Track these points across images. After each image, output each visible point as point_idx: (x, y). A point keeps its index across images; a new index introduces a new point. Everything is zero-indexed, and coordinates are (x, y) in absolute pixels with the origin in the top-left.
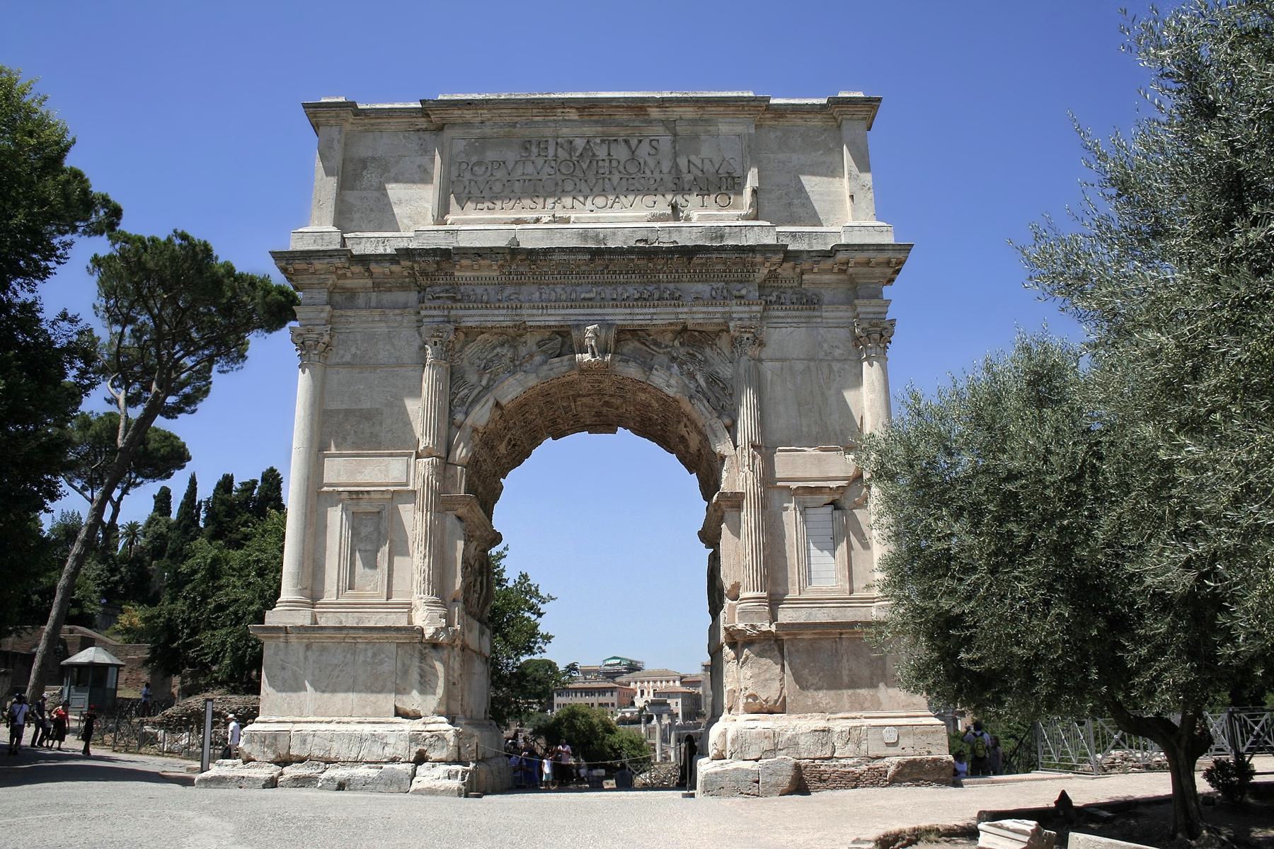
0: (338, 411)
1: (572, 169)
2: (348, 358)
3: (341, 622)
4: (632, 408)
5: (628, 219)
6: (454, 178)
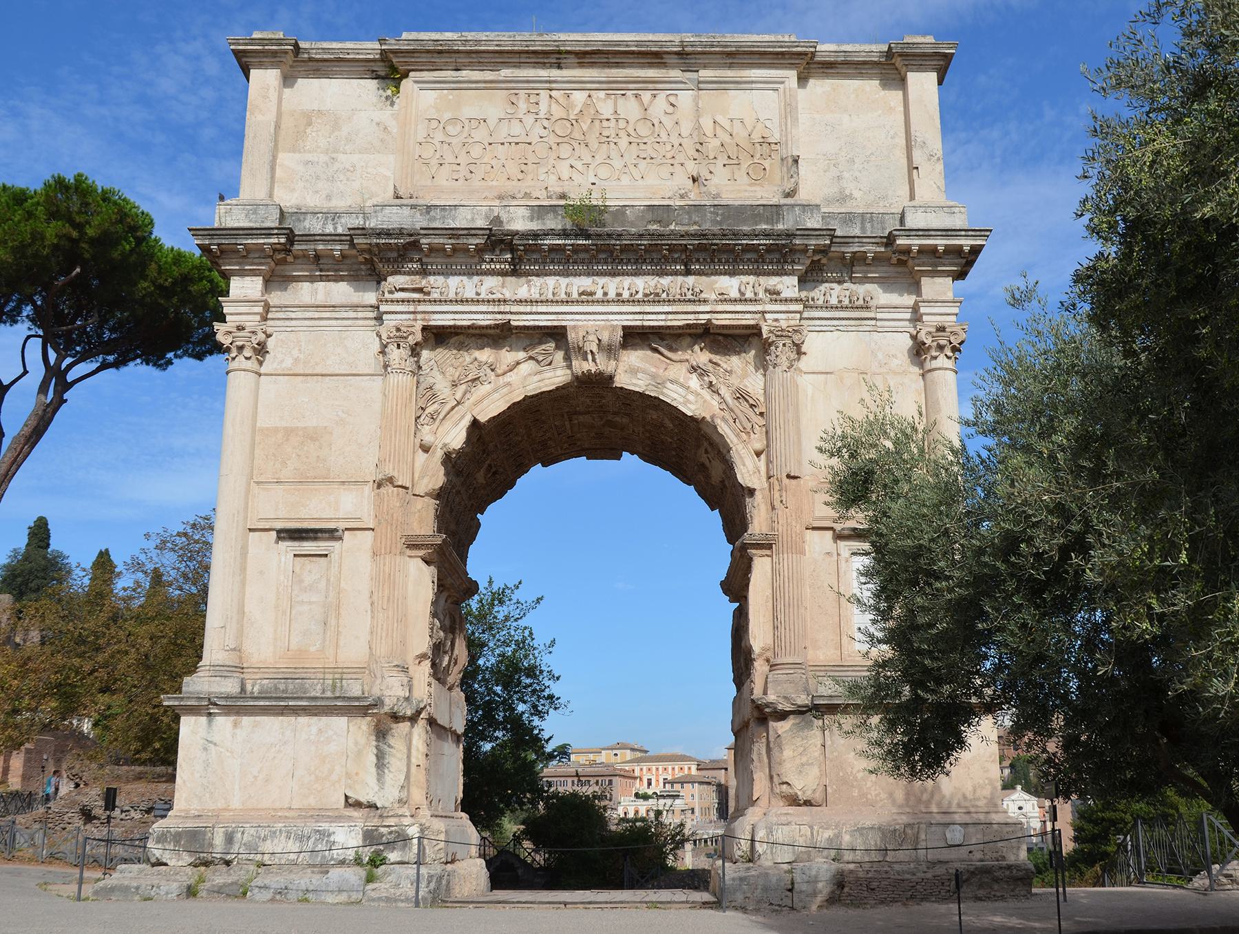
0: (276, 430)
2: (288, 363)
3: (276, 689)
4: (641, 429)
5: (638, 195)
6: (420, 139)
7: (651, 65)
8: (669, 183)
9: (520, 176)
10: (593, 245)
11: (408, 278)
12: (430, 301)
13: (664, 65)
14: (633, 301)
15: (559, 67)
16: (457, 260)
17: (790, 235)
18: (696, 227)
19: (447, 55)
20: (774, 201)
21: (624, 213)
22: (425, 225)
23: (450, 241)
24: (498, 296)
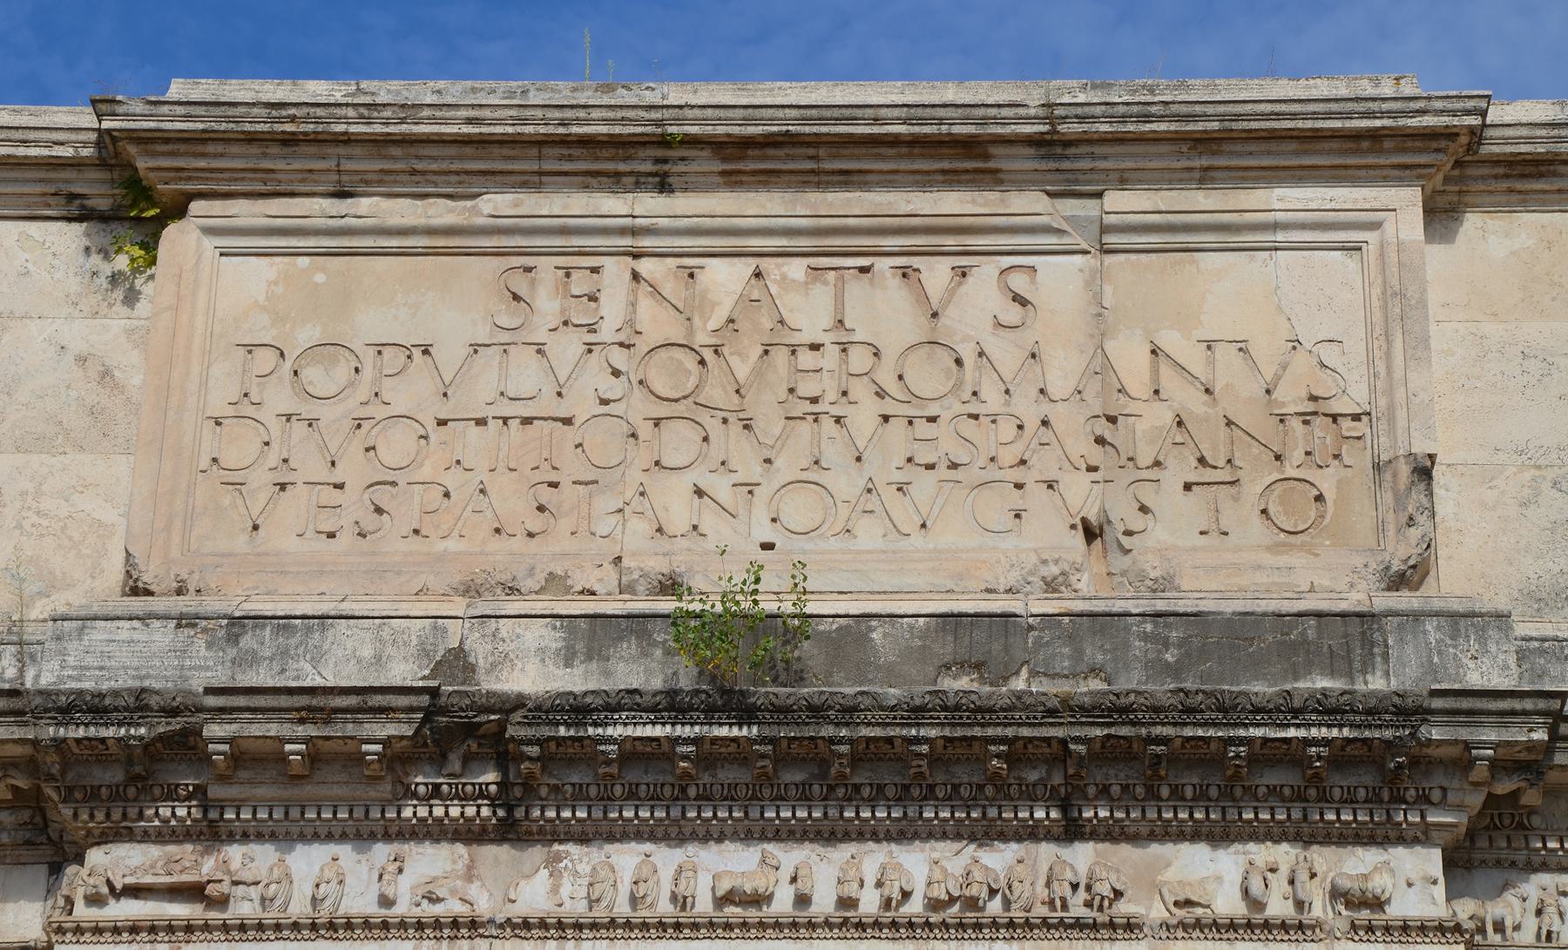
1: (692, 382)
6: (218, 407)
7: (951, 179)
8: (1008, 543)
9: (535, 522)
10: (763, 740)
11: (155, 851)
12: (225, 928)
13: (991, 178)
14: (894, 925)
15: (664, 186)
16: (323, 791)
17: (1408, 711)
18: (1096, 685)
19: (312, 149)
20: (1354, 600)
21: (863, 639)
22: (220, 676)
23: (301, 731)
24: (453, 908)
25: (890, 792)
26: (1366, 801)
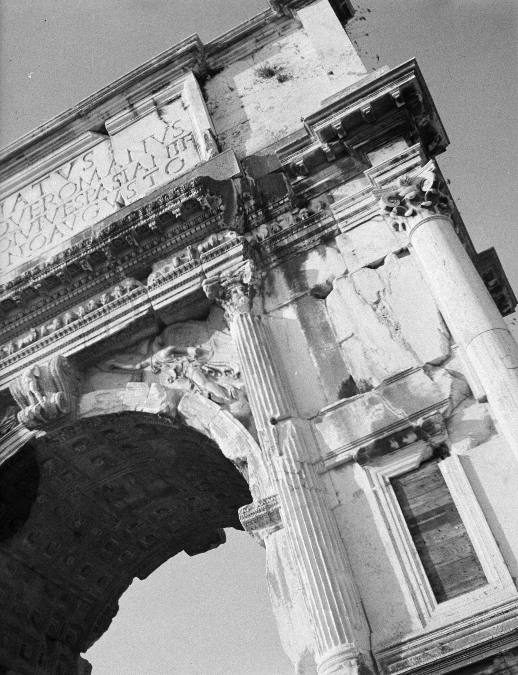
25: (62, 293)
26: (203, 221)
